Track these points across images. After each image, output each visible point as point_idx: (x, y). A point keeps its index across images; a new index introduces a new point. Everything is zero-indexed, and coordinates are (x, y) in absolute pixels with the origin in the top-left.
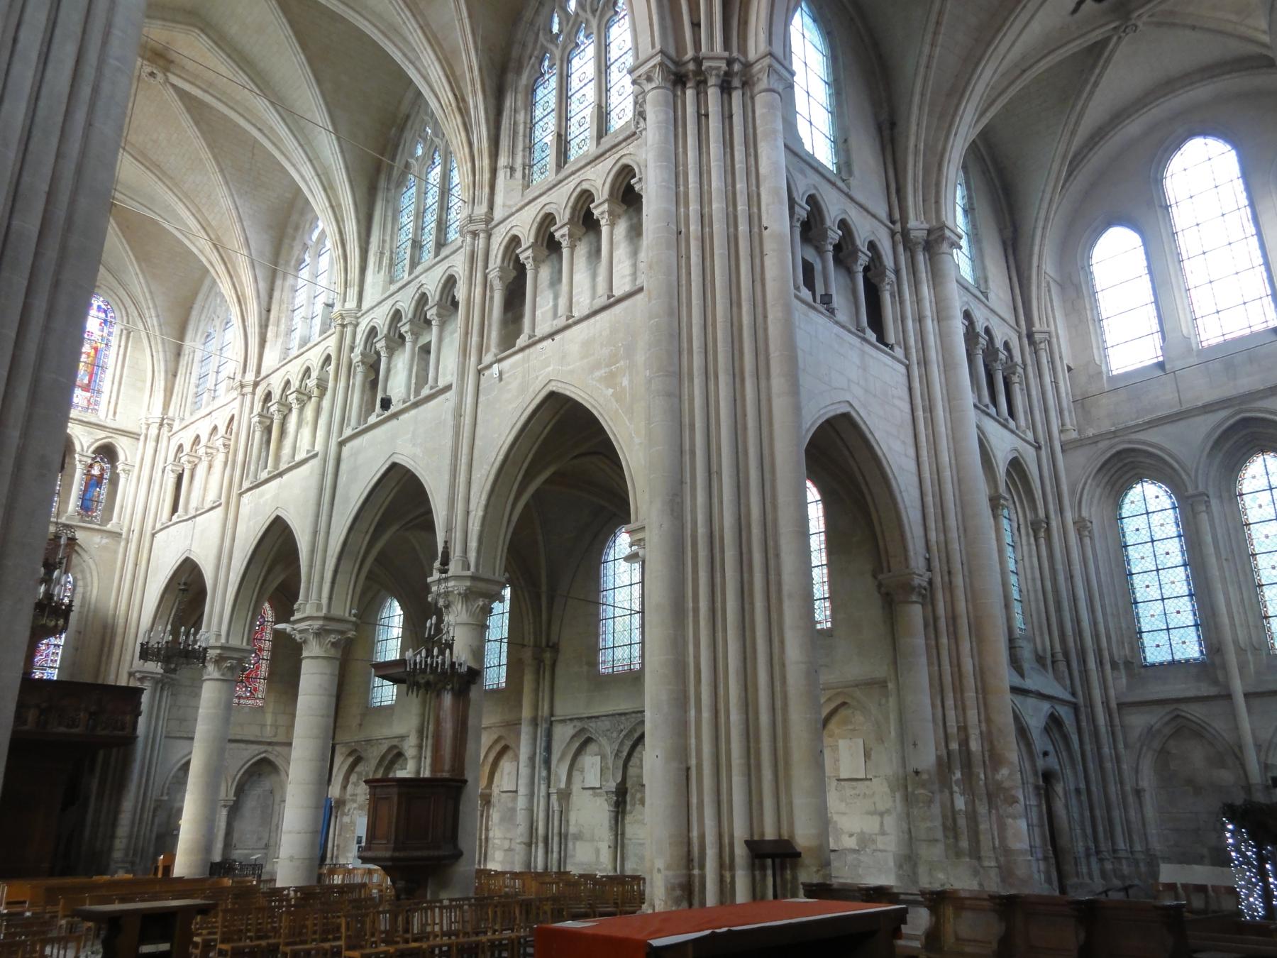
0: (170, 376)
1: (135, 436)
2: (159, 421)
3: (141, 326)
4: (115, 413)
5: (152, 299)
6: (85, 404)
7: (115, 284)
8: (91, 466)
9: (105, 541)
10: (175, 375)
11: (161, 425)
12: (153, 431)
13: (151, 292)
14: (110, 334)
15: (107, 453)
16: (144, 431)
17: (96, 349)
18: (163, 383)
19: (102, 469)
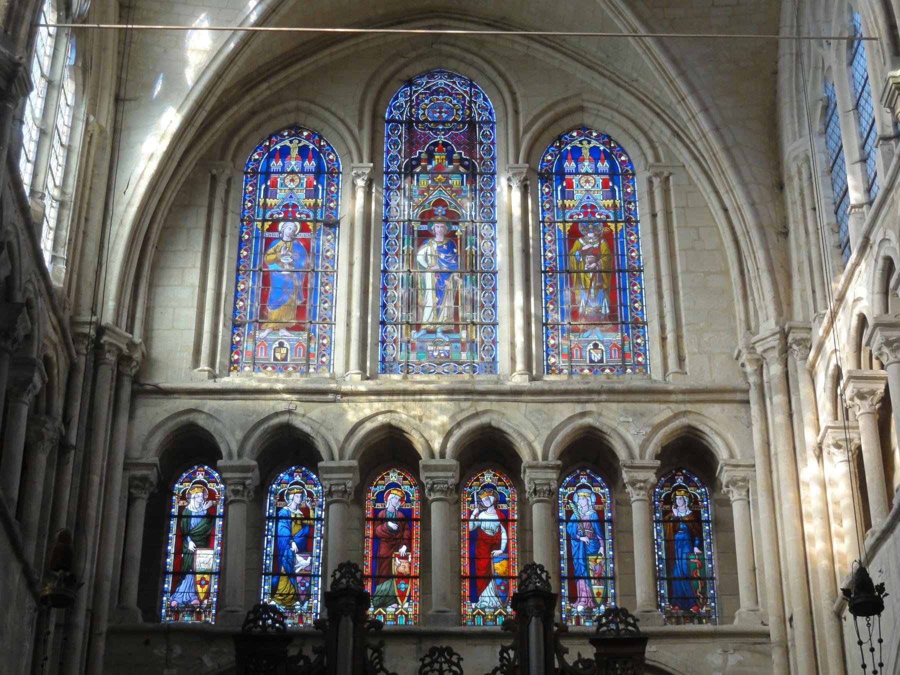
0: (772, 236)
1: (733, 396)
2: (774, 342)
3: (684, 156)
4: (681, 360)
5: (682, 74)
6: (616, 358)
7: (610, 90)
8: (669, 501)
9: (733, 659)
10: (785, 233)
11: (785, 350)
12: (774, 370)
13: (674, 62)
14: (630, 198)
15: (688, 457)
16: (752, 379)
17: (609, 237)
18: (760, 255)
19: (693, 502)
